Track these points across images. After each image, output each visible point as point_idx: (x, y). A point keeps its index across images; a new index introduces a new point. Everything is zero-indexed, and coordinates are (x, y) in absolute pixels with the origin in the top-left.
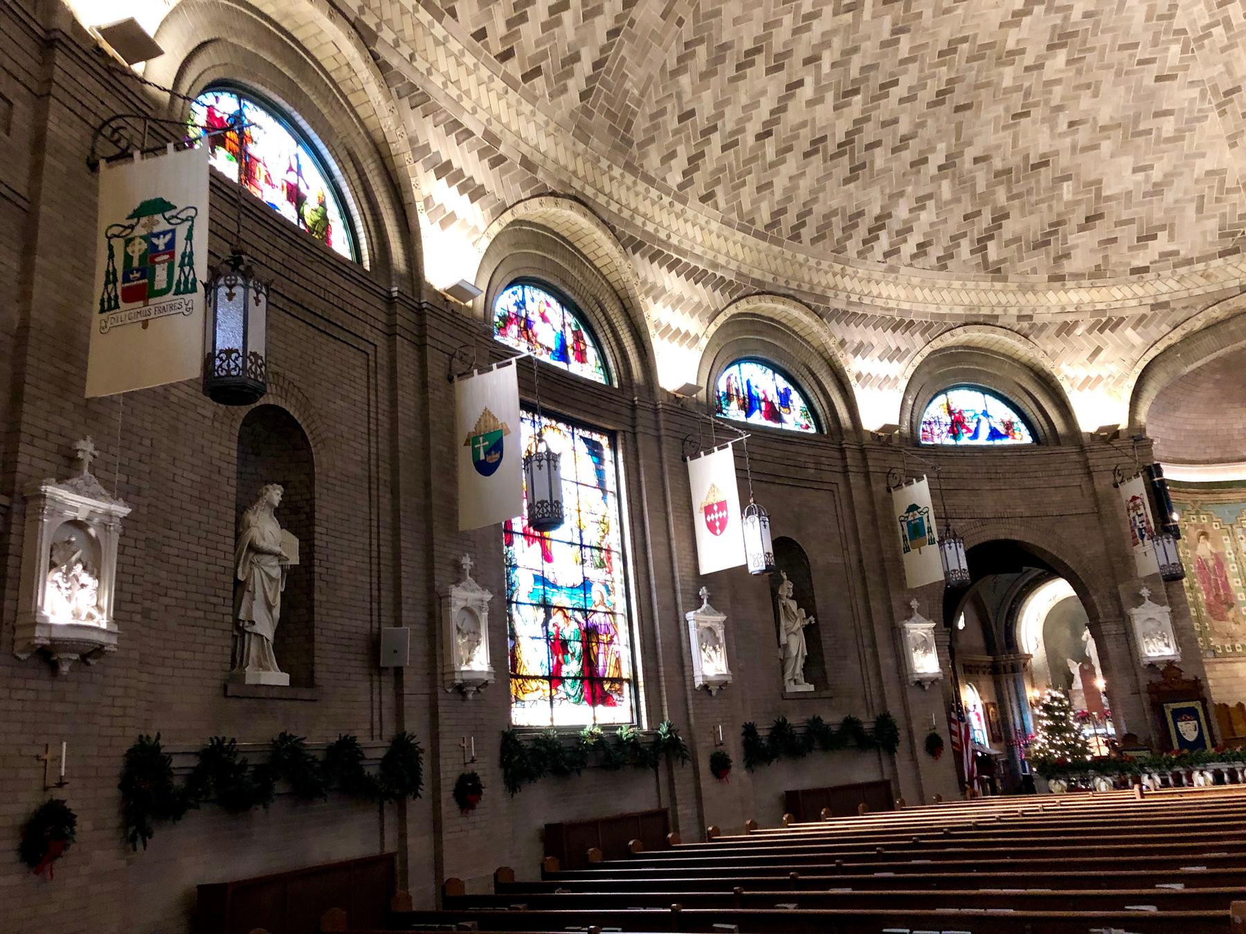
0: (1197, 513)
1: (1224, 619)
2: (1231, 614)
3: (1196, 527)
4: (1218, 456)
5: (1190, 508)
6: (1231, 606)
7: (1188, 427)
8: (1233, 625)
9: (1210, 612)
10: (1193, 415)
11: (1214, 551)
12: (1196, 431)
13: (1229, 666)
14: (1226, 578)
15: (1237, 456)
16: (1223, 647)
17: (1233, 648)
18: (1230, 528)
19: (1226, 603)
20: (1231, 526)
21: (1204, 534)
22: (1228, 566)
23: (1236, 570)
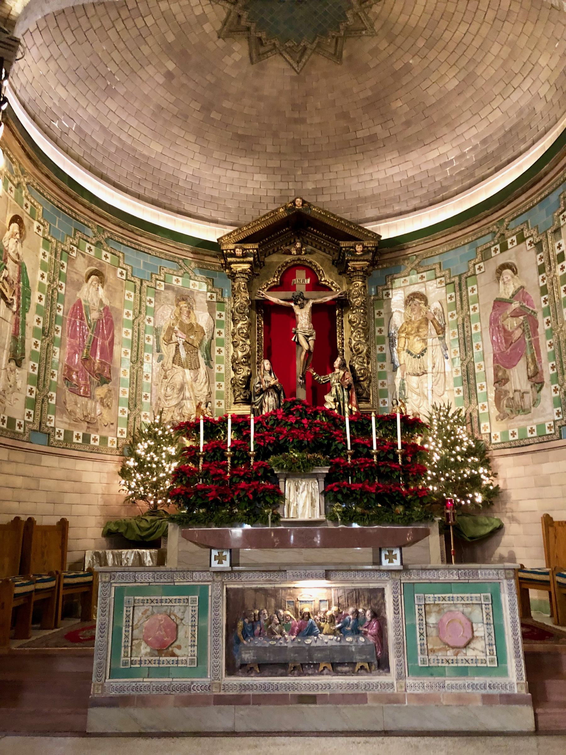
0: (98, 244)
1: (88, 395)
2: (100, 392)
3: (90, 260)
4: (155, 197)
5: (91, 235)
6: (104, 380)
7: (124, 137)
8: (98, 406)
9: (67, 379)
10: (134, 123)
11: (106, 302)
12: (135, 150)
13: (68, 463)
14: (112, 343)
15: (175, 205)
16: (68, 434)
17: (86, 438)
18: (138, 283)
19: (99, 375)
20: (141, 281)
21: (97, 273)
22: (120, 330)
23: (130, 337)
